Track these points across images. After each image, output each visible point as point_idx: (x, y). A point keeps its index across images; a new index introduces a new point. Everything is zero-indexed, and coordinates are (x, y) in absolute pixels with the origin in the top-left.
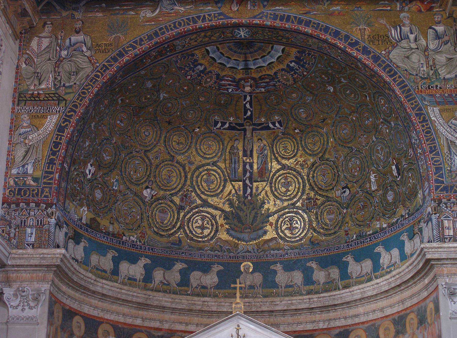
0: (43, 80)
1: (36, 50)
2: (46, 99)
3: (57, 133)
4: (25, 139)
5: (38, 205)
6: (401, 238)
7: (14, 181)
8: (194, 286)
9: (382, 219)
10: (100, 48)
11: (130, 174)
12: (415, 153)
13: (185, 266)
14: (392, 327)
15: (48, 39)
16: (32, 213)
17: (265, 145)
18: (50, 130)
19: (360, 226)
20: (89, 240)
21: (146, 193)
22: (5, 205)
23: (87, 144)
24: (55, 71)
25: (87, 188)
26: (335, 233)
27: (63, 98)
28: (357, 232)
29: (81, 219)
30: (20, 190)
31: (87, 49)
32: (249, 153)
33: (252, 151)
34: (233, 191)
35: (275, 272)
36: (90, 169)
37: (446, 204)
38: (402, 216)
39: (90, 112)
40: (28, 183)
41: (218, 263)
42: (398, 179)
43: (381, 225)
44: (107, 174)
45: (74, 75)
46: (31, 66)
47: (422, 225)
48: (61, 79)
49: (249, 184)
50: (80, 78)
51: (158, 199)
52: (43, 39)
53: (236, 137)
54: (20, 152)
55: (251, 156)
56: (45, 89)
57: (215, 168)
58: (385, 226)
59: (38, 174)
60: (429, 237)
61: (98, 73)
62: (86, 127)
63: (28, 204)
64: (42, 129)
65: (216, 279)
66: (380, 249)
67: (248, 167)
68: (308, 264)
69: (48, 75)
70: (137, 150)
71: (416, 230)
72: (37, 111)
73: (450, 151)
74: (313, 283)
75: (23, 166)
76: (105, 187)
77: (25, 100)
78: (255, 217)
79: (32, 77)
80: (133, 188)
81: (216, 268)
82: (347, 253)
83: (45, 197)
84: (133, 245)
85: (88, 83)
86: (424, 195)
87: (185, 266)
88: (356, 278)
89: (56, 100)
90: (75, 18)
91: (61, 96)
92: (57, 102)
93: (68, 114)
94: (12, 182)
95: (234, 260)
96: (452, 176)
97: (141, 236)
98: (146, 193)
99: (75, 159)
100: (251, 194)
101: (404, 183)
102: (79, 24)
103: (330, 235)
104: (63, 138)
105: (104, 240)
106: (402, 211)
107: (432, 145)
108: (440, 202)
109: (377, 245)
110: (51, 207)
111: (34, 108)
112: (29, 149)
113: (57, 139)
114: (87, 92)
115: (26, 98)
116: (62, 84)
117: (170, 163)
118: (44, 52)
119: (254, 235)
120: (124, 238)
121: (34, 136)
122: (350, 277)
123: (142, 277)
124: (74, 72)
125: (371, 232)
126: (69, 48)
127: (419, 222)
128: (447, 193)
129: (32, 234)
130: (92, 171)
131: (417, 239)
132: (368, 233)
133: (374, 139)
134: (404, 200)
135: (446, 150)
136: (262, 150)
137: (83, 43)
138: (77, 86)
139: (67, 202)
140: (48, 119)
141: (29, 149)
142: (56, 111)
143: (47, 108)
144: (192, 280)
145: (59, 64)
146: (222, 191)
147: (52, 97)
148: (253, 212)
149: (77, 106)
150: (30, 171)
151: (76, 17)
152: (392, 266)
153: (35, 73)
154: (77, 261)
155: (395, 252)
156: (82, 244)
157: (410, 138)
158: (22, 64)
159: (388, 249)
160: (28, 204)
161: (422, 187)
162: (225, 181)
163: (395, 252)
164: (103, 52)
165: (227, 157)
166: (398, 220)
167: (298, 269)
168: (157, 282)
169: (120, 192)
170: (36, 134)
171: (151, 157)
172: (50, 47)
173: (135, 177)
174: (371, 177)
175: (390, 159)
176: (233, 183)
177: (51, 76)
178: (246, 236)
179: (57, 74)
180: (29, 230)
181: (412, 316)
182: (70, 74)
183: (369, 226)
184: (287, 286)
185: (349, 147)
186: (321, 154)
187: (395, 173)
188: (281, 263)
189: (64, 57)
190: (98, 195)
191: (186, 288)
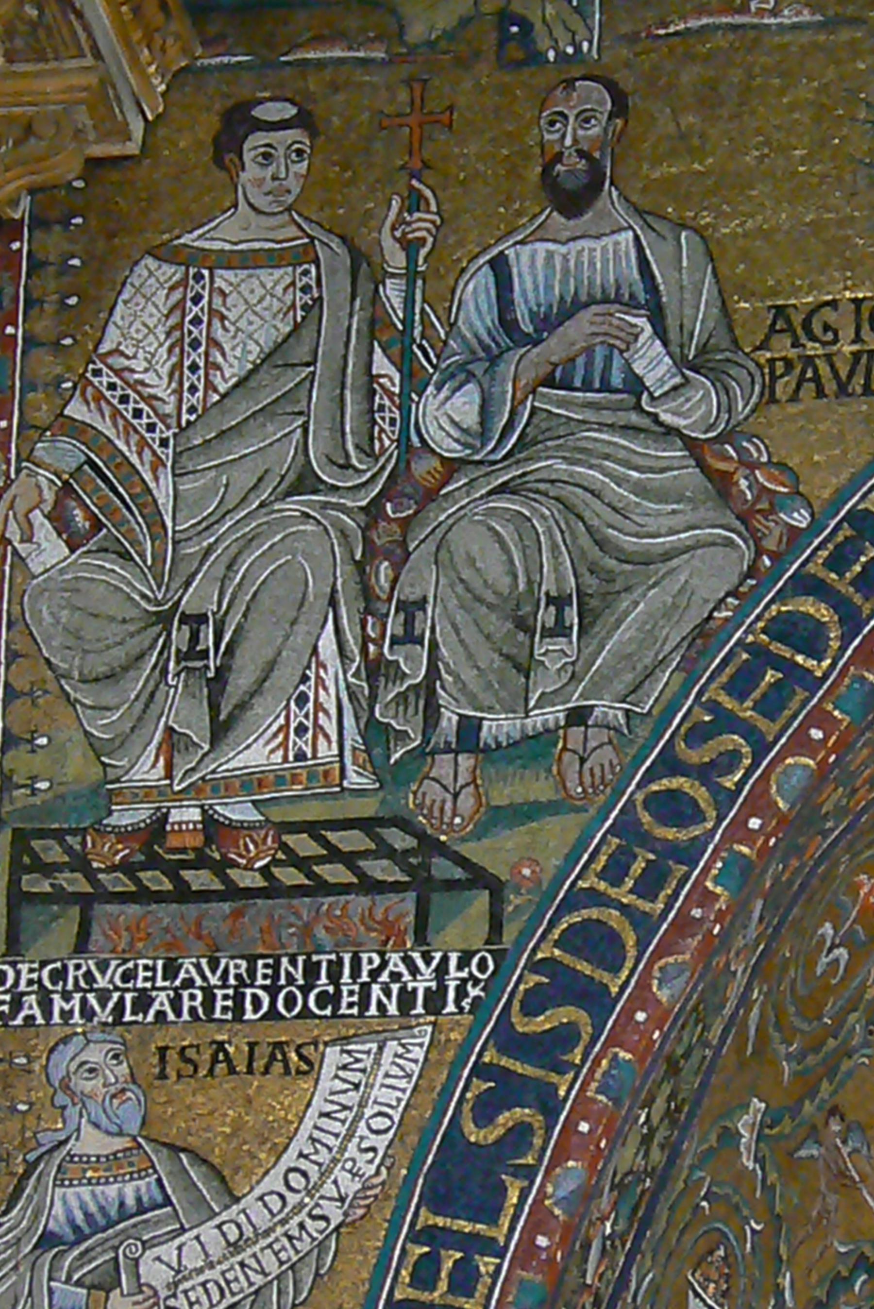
0: (256, 691)
1: (161, 387)
2: (290, 876)
3: (427, 1218)
10: (813, 349)
15: (280, 276)
18: (351, 1186)
24: (367, 593)
27: (462, 861)
31: (681, 363)
39: (733, 993)
45: (560, 630)
46: (125, 556)
48: (433, 672)
50: (625, 658)
52: (224, 278)
56: (280, 780)
61: (808, 606)
62: (691, 1149)
64: (274, 1182)
69: (300, 639)
72: (209, 994)
77: (85, 901)
79: (141, 657)
85: (714, 707)
89: (396, 887)
90: (536, 58)
91: (442, 849)
92: (408, 903)
93: (522, 1025)
102: (585, 119)
104: (486, 1264)
111: (171, 971)
114: (701, 795)
115: (90, 875)
116: (449, 720)
118: (244, 408)
121: (193, 1260)
124: (559, 602)
126: (494, 360)
137: (632, 304)
138: (596, 737)
140: (326, 1083)
142: (407, 999)
143: (312, 971)
145: (405, 523)
147: (349, 859)
149: (614, 938)
151: (543, 42)
153: (164, 619)
158: (28, 538)
164: (843, 389)
170: (208, 1231)
172: (302, 353)
177: (327, 644)
179: (394, 625)
182: (524, 625)
189: (452, 449)
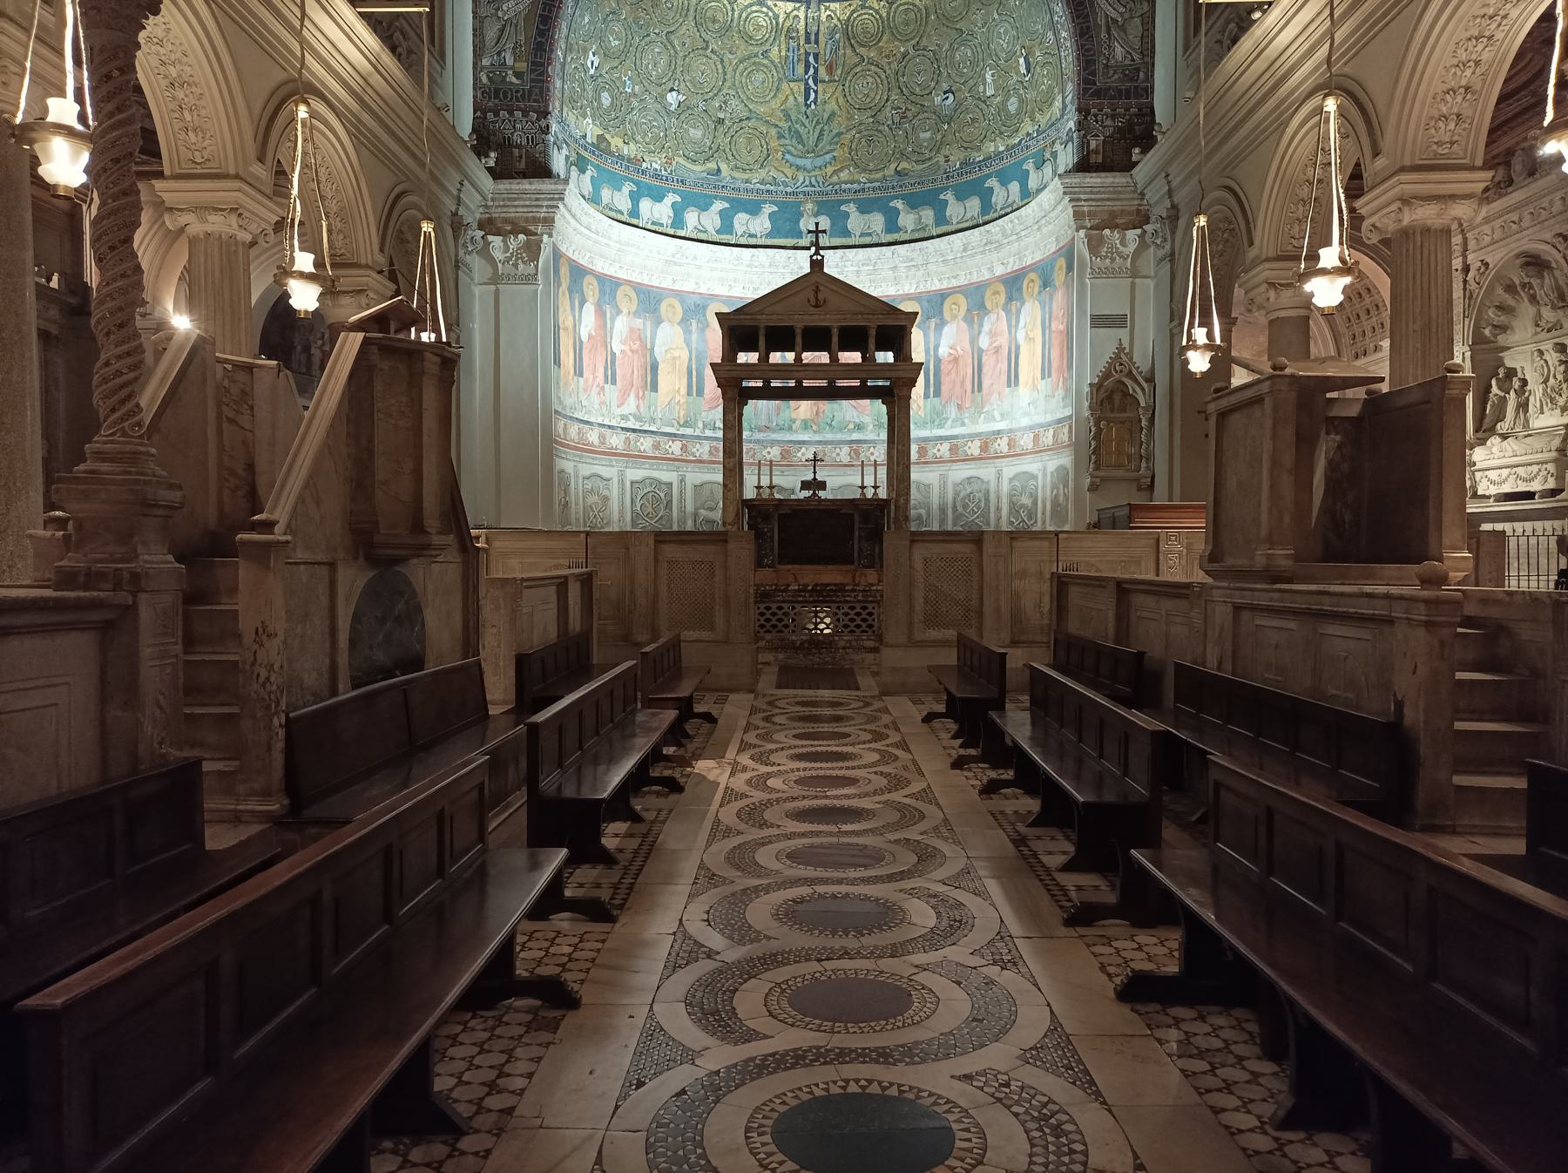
4: (497, 10)
5: (526, 114)
6: (1025, 167)
7: (488, 76)
8: (739, 234)
9: (998, 139)
11: (647, 66)
12: (1057, 40)
13: (727, 205)
14: (1001, 288)
16: (518, 126)
17: (836, 26)
19: (966, 149)
20: (597, 167)
21: (672, 98)
22: (479, 114)
23: (587, 20)
25: (589, 88)
26: (930, 159)
28: (962, 158)
29: (585, 137)
30: (497, 91)
32: (813, 38)
33: (817, 34)
34: (791, 98)
35: (847, 215)
36: (592, 59)
37: (1095, 116)
38: (1028, 134)
40: (508, 80)
41: (771, 202)
42: (1027, 79)
43: (996, 147)
44: (616, 67)
47: (1058, 147)
49: (813, 86)
51: (688, 108)
53: (795, 13)
54: (491, 33)
55: (817, 42)
57: (765, 62)
58: (1002, 148)
59: (522, 66)
60: (1067, 165)
63: (511, 113)
65: (768, 225)
66: (992, 183)
67: (811, 59)
68: (891, 204)
70: (657, 31)
71: (1047, 155)
73: (1109, 34)
74: (898, 230)
75: (499, 54)
76: (615, 88)
78: (821, 134)
80: (655, 91)
81: (768, 209)
82: (946, 189)
83: (535, 101)
84: (657, 176)
86: (1063, 102)
87: (727, 205)
88: (958, 223)
94: (485, 80)
95: (792, 199)
96: (1108, 73)
97: (666, 163)
98: (672, 98)
99: (571, 45)
100: (815, 101)
101: (1034, 84)
103: (924, 162)
105: (617, 169)
106: (1028, 127)
107: (1084, 25)
108: (1088, 113)
109: (989, 176)
110: (545, 118)
112: (504, 26)
113: (544, 10)
117: (701, 52)
119: (819, 162)
120: (644, 165)
122: (948, 223)
123: (670, 222)
125: (982, 158)
127: (1053, 143)
128: (1099, 98)
129: (521, 157)
130: (596, 64)
131: (1048, 169)
132: (978, 159)
133: (996, 17)
134: (1033, 112)
135: (1103, 34)
136: (833, 31)
139: (565, 109)
141: (504, 26)
144: (736, 225)
146: (775, 96)
148: (819, 127)
150: (510, 61)
152: (1008, 206)
154: (584, 197)
155: (1015, 187)
156: (589, 173)
157: (1051, 12)
159: (1004, 183)
160: (511, 113)
161: (1063, 91)
162: (780, 79)
163: (1015, 187)
165: (783, 46)
166: (1021, 140)
167: (879, 210)
168: (690, 228)
169: (635, 95)
171: (676, 43)
173: (654, 73)
174: (987, 76)
175: (1018, 47)
176: (792, 84)
178: (807, 163)
180: (516, 152)
181: (1033, 276)
183: (979, 149)
184: (862, 235)
185: (957, 29)
186: (914, 42)
187: (1023, 70)
188: (854, 200)
190: (606, 99)
191: (729, 237)
